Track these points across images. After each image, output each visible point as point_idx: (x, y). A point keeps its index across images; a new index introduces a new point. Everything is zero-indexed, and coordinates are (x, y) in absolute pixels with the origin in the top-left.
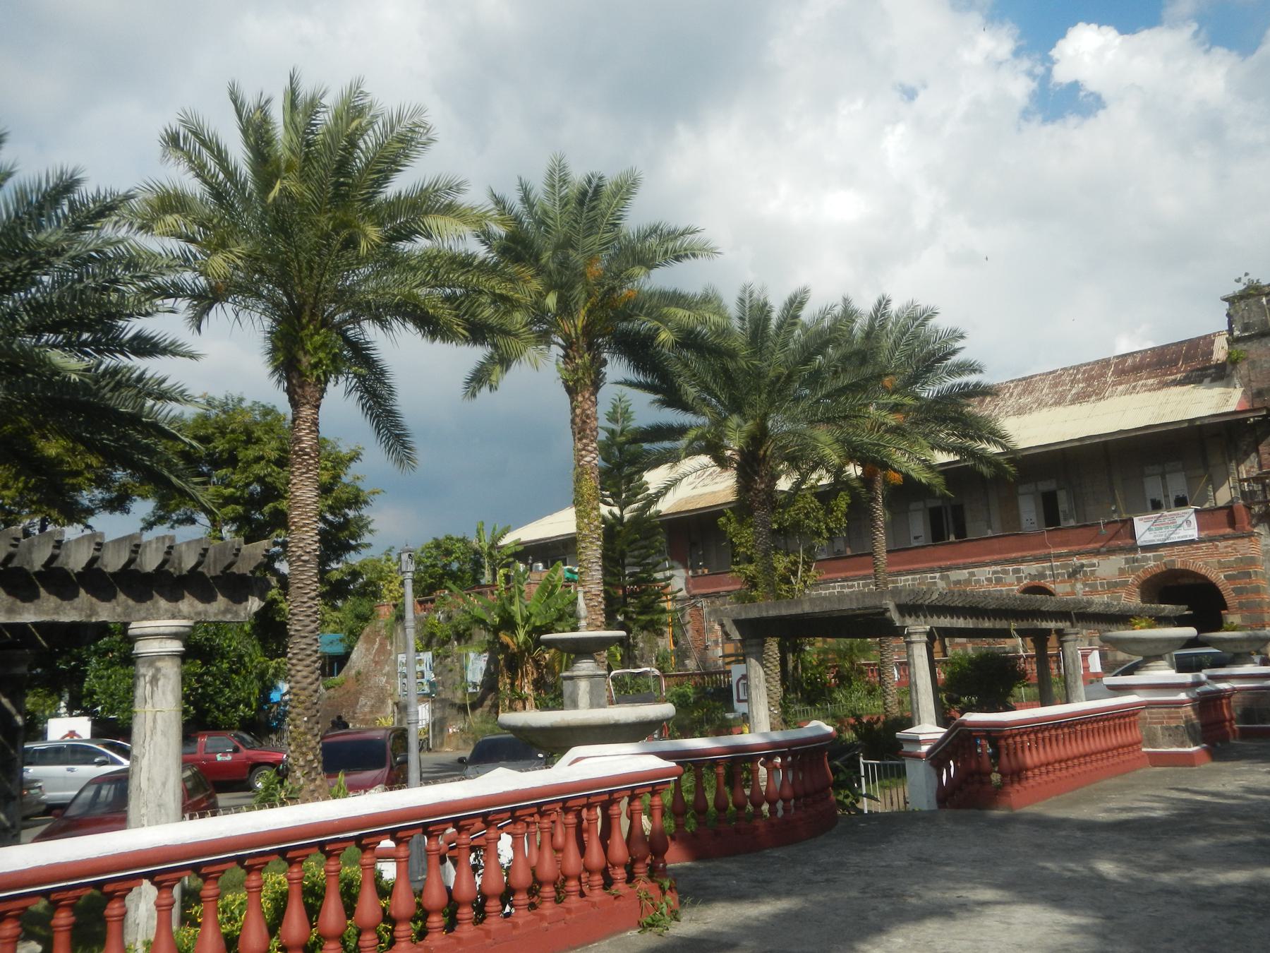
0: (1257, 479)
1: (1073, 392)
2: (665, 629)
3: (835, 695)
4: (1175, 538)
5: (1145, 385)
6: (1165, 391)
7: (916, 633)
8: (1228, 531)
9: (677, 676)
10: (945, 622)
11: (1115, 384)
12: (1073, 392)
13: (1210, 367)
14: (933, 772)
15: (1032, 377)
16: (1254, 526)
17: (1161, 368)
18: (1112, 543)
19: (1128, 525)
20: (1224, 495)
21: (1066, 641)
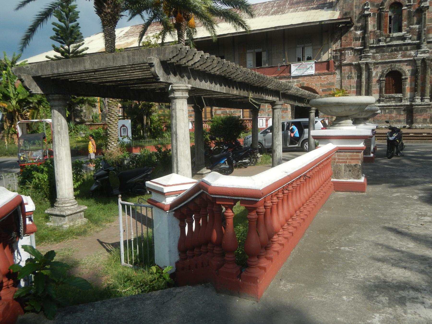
0: (340, 51)
1: (272, 10)
2: (96, 104)
3: (164, 134)
4: (306, 73)
5: (301, 9)
6: (309, 11)
7: (178, 90)
8: (326, 71)
9: (102, 124)
10: (205, 85)
11: (289, 8)
12: (272, 10)
13: (327, 3)
14: (176, 222)
15: (256, 4)
16: (335, 70)
17: (307, 3)
18: (282, 75)
19: (289, 68)
20: (325, 57)
21: (275, 109)
